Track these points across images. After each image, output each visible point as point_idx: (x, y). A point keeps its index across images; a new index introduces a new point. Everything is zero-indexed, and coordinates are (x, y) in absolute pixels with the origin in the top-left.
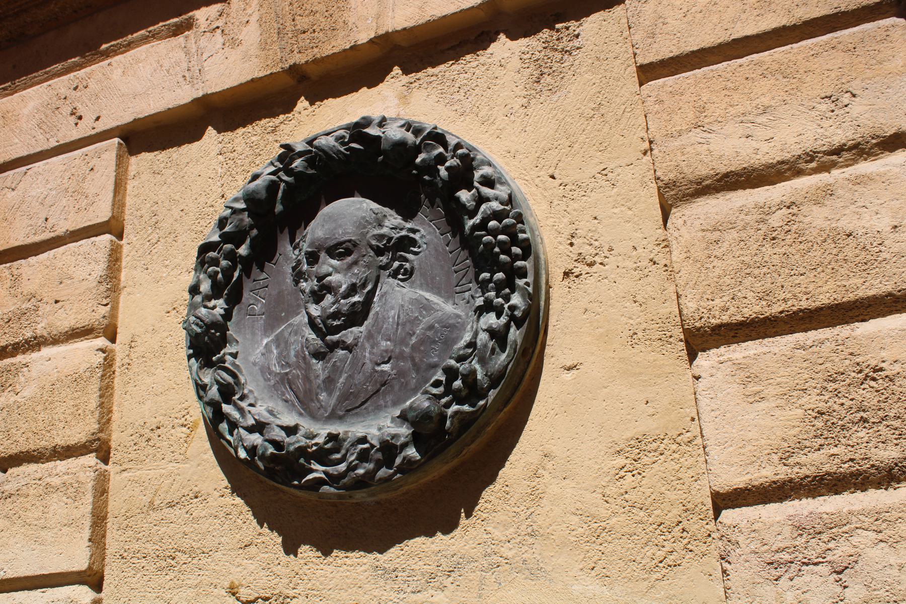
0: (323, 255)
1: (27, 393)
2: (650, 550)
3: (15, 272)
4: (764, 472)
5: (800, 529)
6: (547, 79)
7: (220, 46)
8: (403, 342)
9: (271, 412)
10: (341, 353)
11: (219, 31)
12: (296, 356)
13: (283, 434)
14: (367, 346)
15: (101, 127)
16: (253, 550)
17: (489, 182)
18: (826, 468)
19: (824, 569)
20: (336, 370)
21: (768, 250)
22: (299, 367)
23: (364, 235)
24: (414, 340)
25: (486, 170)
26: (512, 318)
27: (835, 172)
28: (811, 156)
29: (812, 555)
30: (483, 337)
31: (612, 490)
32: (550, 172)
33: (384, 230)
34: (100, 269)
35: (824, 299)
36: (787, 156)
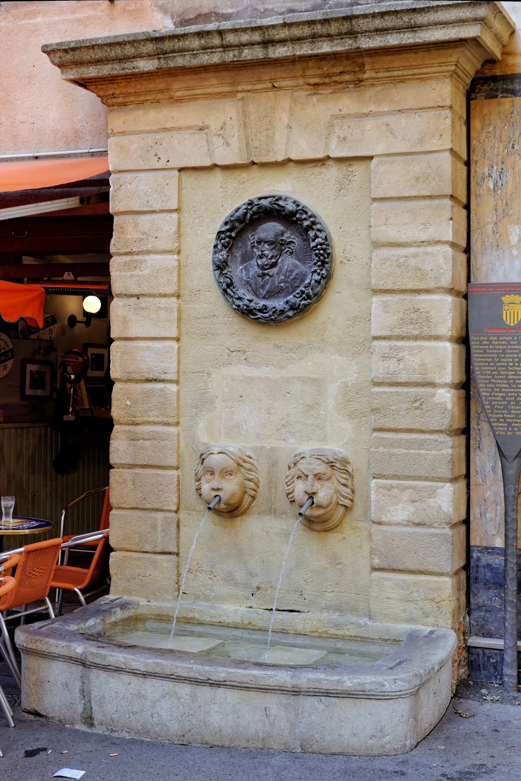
0: (263, 243)
1: (147, 271)
2: (354, 349)
3: (136, 222)
4: (385, 333)
5: (391, 348)
6: (343, 191)
7: (221, 144)
8: (288, 277)
9: (244, 294)
10: (268, 277)
12: (252, 276)
13: (248, 302)
14: (277, 277)
15: (170, 165)
16: (235, 336)
17: (320, 231)
18: (400, 334)
20: (266, 283)
21: (397, 270)
22: (253, 279)
23: (277, 239)
24: (291, 277)
25: (318, 226)
26: (322, 277)
27: (422, 248)
28: (415, 242)
29: (393, 355)
30: (313, 282)
31: (346, 331)
32: (340, 226)
33: (284, 238)
34: (174, 228)
35: (409, 287)
36: (409, 241)
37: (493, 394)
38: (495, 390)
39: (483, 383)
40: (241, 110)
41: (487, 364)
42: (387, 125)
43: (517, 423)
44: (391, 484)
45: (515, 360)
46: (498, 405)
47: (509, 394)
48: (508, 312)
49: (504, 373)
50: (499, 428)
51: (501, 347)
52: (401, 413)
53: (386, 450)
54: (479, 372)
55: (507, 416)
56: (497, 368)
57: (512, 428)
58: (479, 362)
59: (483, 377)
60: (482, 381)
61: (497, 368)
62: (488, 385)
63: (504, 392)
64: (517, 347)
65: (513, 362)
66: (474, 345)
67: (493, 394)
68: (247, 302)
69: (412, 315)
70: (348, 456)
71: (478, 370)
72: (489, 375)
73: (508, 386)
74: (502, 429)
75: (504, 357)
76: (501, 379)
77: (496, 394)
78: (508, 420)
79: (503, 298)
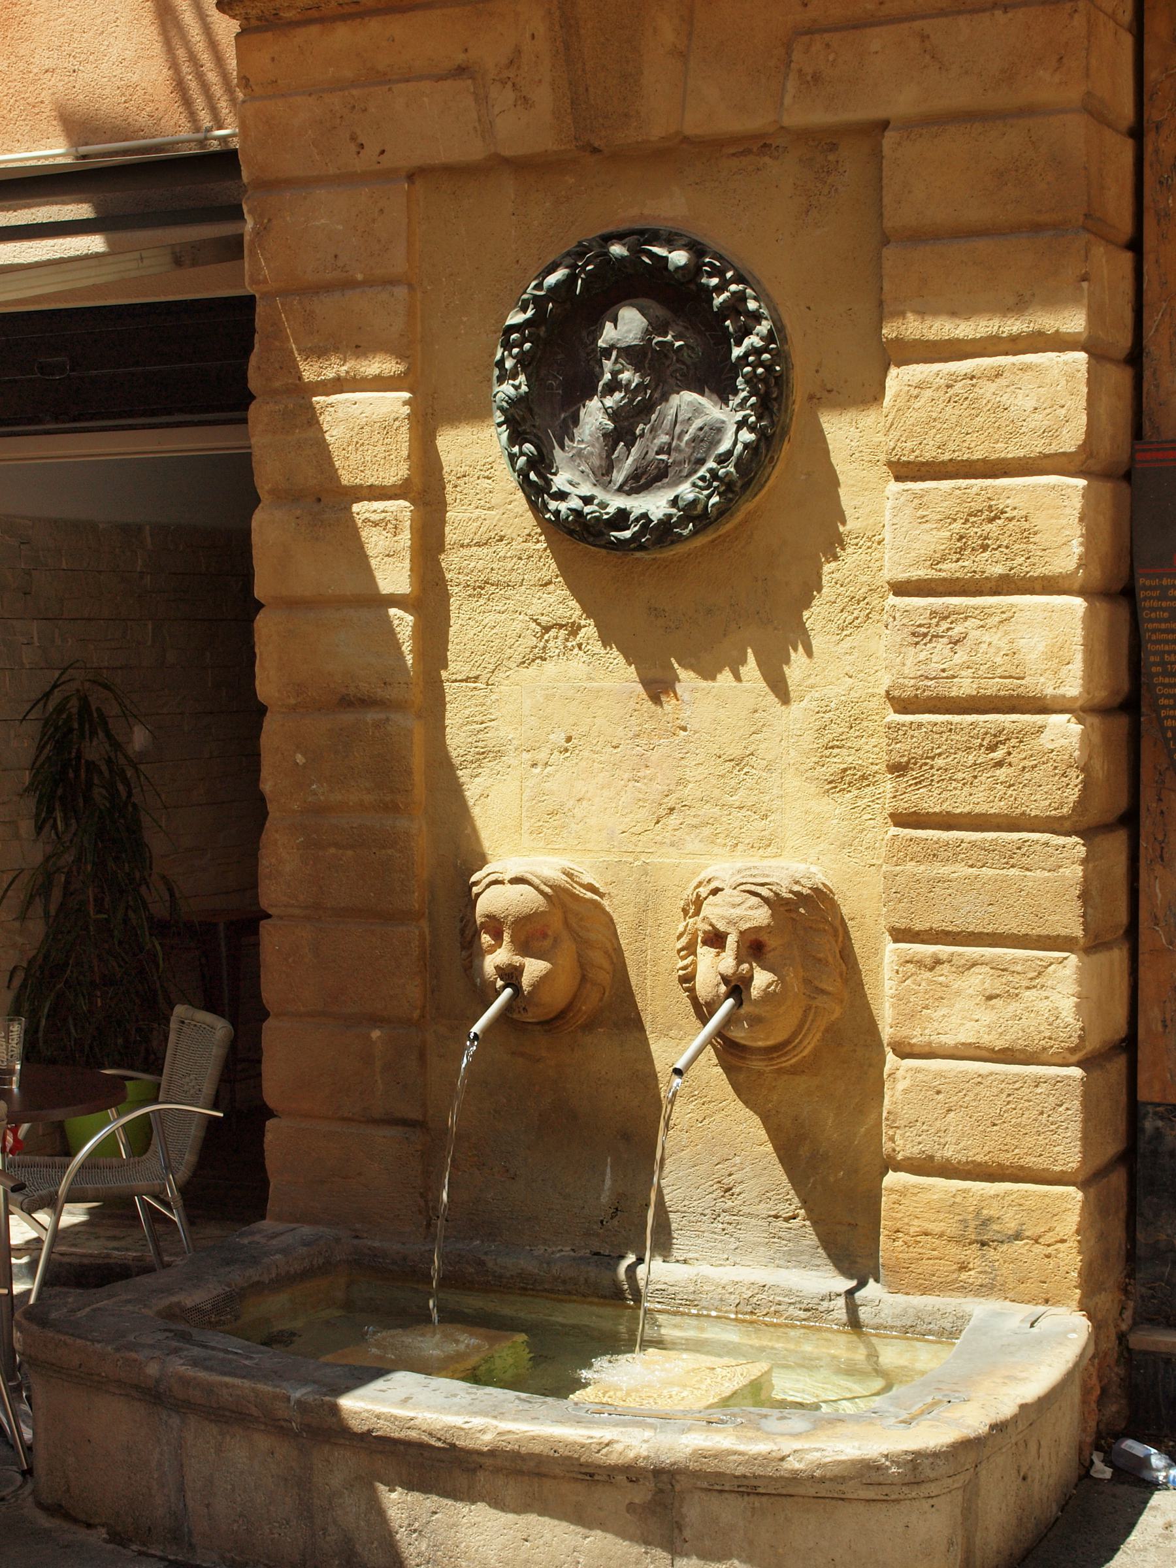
5: (934, 614)
8: (680, 437)
11: (510, 84)
13: (581, 503)
15: (387, 162)
16: (551, 587)
18: (958, 574)
19: (945, 640)
23: (650, 340)
40: (557, 13)
42: (924, 38)
44: (934, 953)
52: (960, 776)
53: (922, 868)
54: (1159, 669)
59: (1167, 680)
60: (1166, 691)
68: (575, 503)
69: (988, 527)
70: (829, 884)
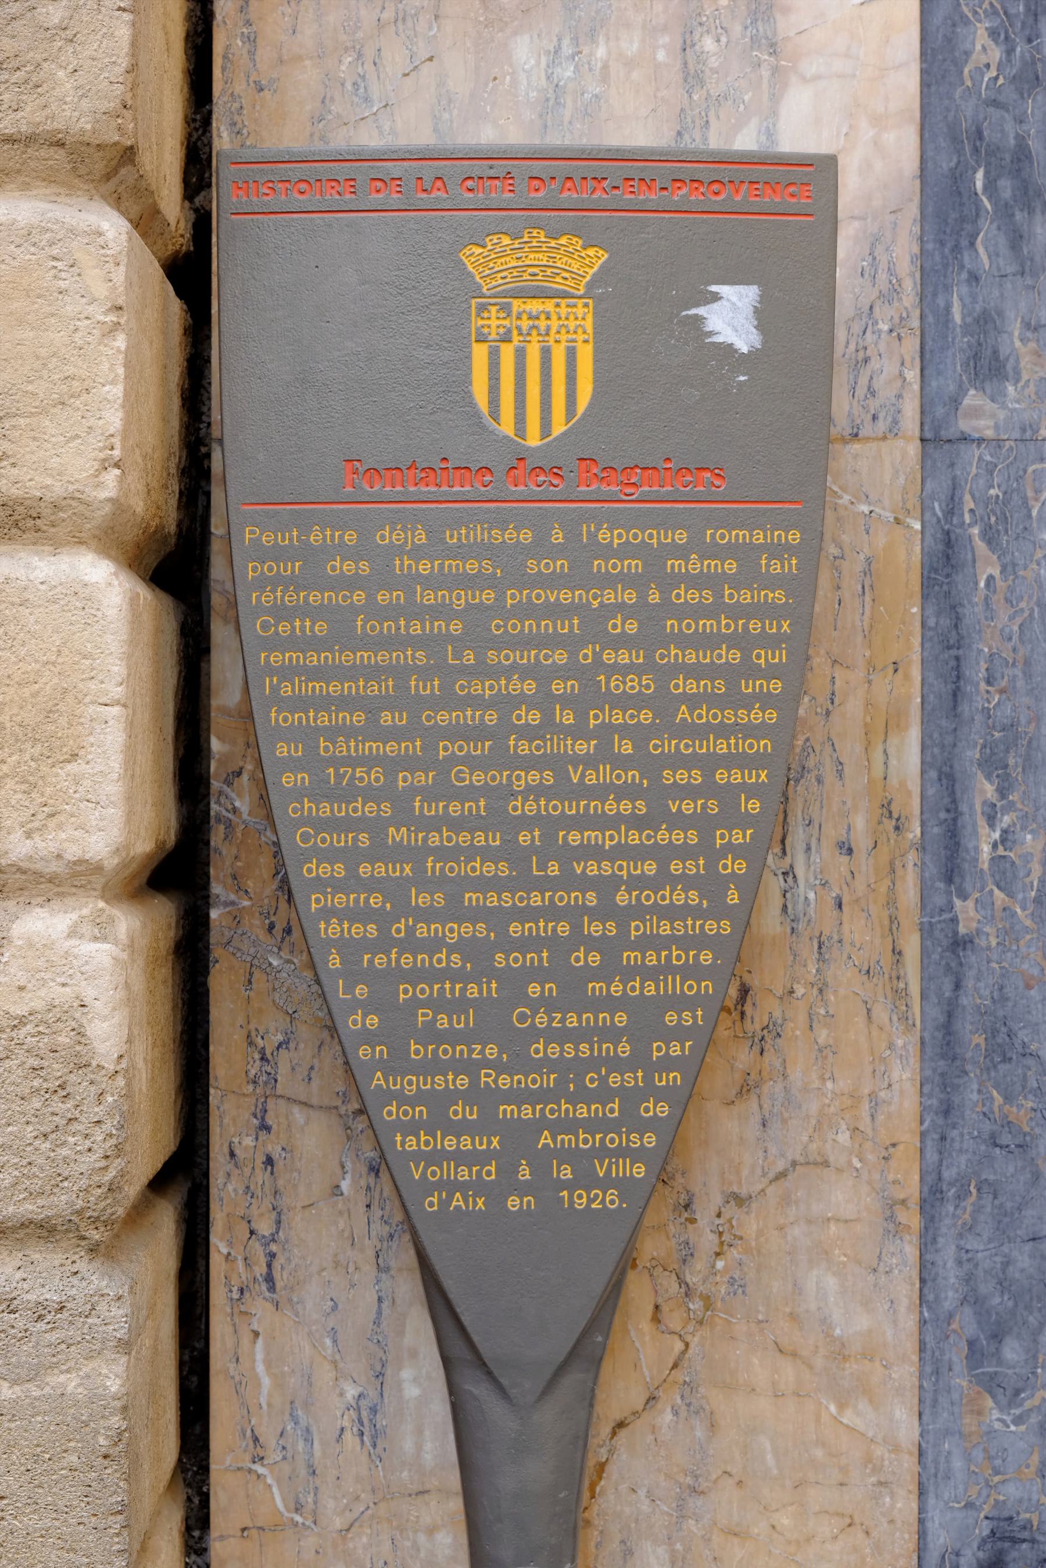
37: (399, 928)
38: (422, 900)
39: (331, 856)
41: (358, 718)
43: (570, 1126)
45: (557, 687)
46: (438, 1005)
47: (515, 929)
48: (507, 353)
49: (478, 778)
50: (447, 1171)
51: (460, 599)
55: (505, 1082)
56: (430, 747)
57: (541, 1162)
58: (301, 704)
59: (326, 810)
61: (430, 747)
62: (364, 870)
63: (475, 915)
64: (565, 596)
65: (545, 701)
66: (261, 583)
67: (399, 928)
71: (294, 765)
72: (370, 794)
73: (504, 869)
74: (464, 1174)
75: (482, 671)
76: (457, 825)
77: (422, 931)
78: (507, 1110)
79: (471, 257)
